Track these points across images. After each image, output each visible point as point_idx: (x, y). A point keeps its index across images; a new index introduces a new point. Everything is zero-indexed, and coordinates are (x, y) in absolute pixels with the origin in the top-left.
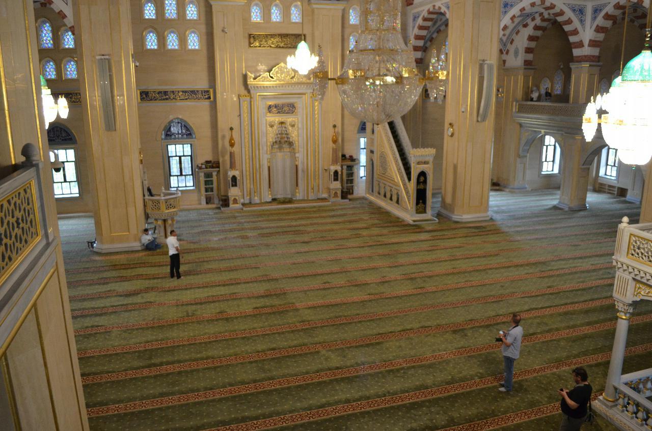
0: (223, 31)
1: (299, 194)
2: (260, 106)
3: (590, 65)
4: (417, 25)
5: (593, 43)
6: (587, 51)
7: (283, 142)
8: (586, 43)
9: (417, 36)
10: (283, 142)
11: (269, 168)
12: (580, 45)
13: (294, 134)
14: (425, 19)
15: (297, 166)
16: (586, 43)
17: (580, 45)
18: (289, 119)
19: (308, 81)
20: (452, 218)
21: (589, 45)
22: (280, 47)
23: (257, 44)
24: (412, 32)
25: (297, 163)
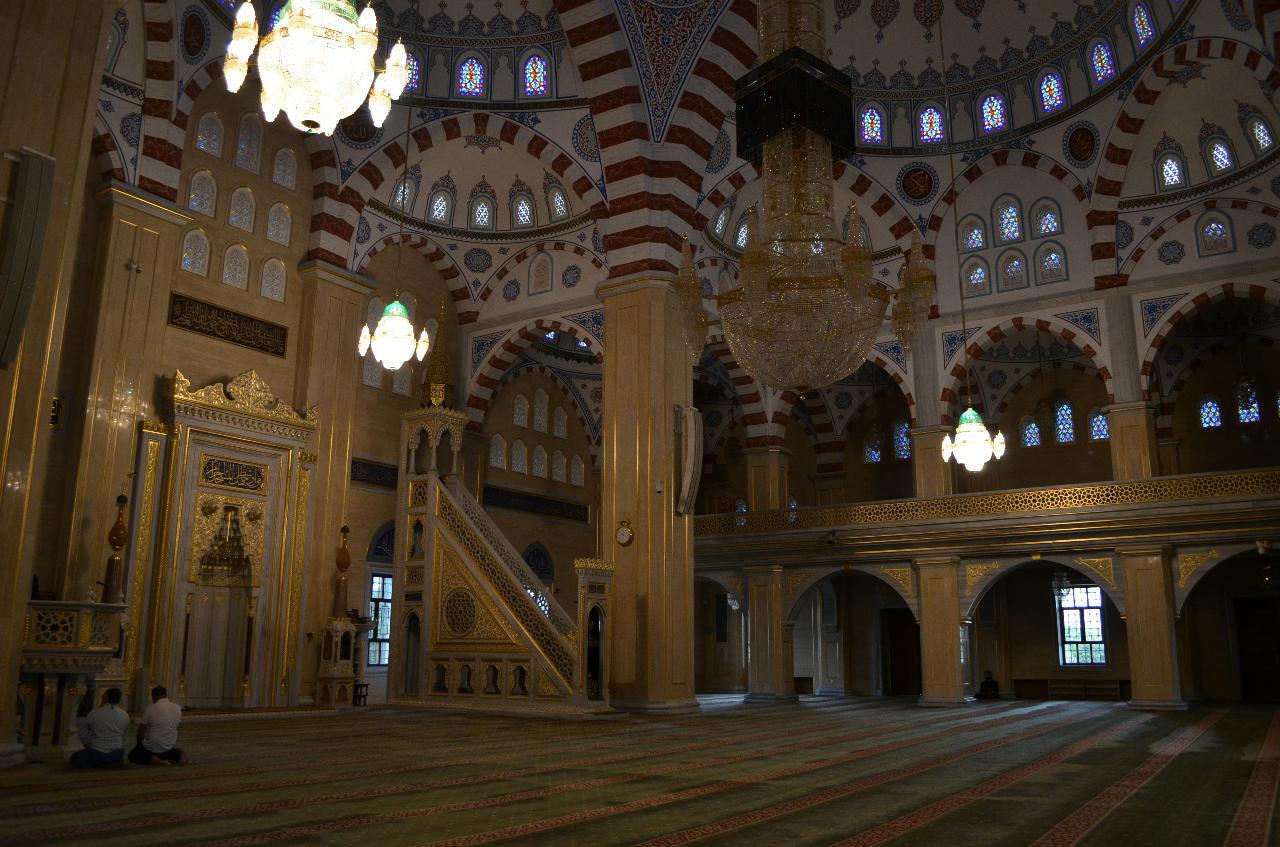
0: (128, 267)
1: (251, 693)
2: (190, 456)
3: (781, 452)
4: (489, 357)
5: (779, 418)
6: (771, 429)
7: (229, 557)
8: (770, 417)
9: (486, 378)
10: (229, 557)
11: (188, 616)
12: (760, 418)
13: (254, 541)
14: (509, 347)
15: (250, 620)
16: (770, 417)
17: (760, 418)
18: (247, 503)
19: (301, 421)
20: (645, 709)
21: (774, 421)
22: (234, 340)
23: (188, 322)
24: (475, 368)
25: (252, 612)
